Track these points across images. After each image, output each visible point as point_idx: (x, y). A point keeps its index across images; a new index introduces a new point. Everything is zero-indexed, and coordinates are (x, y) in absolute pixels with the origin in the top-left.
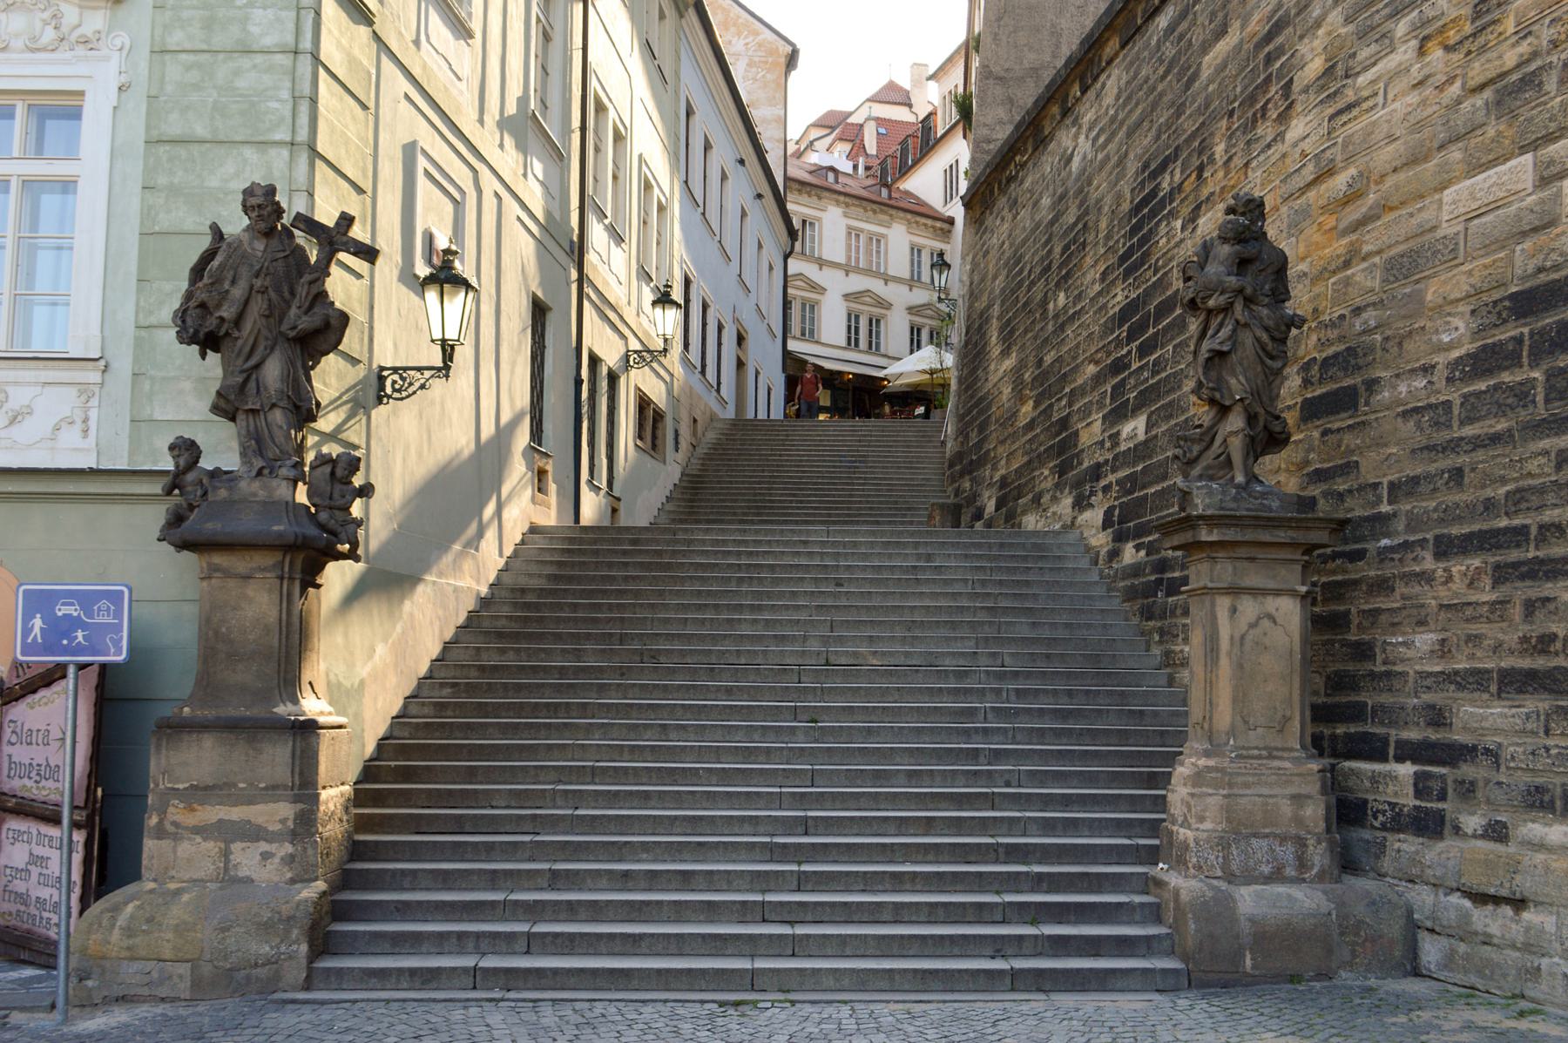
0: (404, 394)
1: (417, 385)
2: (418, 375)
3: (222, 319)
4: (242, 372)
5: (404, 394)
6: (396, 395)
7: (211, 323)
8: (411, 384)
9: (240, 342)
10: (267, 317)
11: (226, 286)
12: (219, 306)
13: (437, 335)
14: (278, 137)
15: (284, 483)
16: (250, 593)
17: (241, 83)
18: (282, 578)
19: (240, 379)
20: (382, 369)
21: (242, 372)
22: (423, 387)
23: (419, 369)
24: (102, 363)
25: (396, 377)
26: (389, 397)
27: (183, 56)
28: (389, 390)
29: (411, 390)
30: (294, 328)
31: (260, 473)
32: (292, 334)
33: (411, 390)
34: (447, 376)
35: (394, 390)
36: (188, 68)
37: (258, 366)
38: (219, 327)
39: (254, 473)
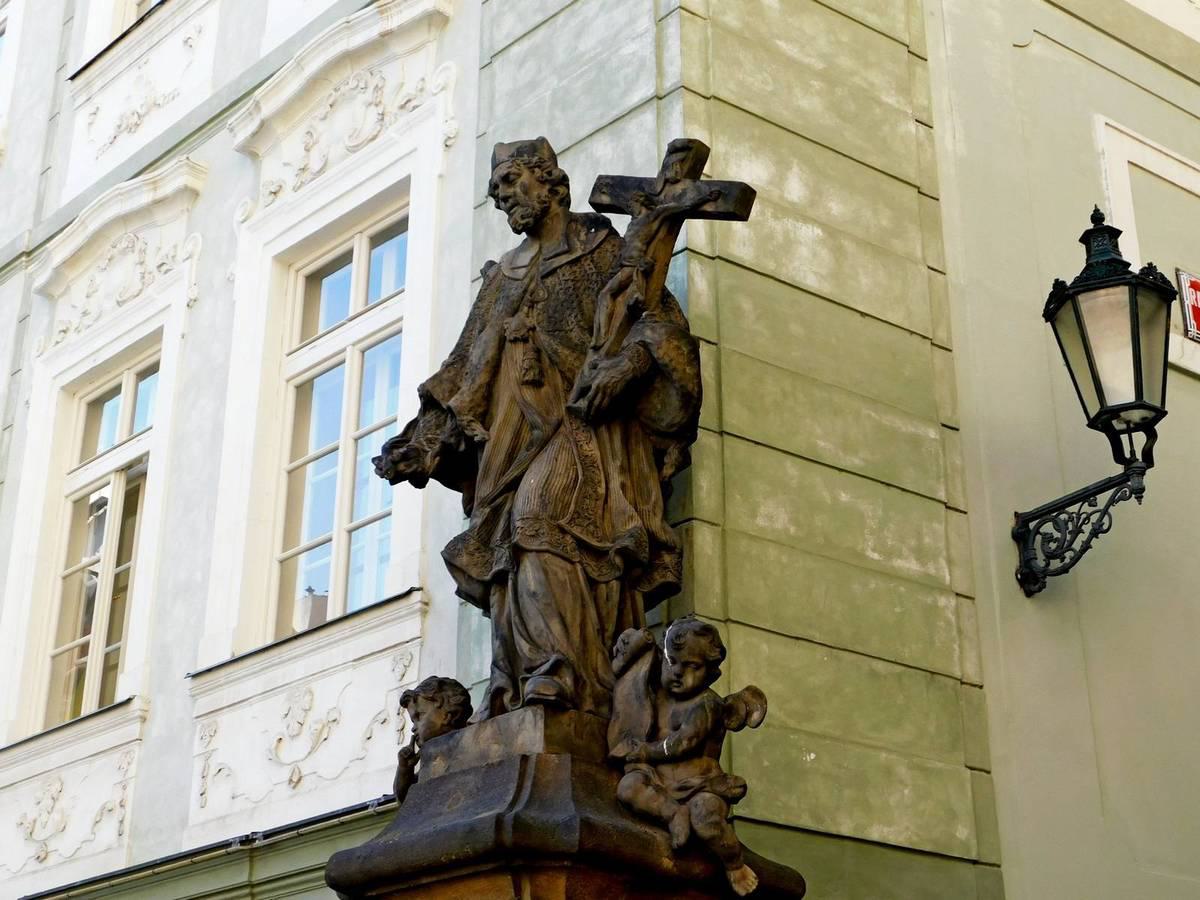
0: (1069, 555)
1: (1087, 528)
2: (1086, 508)
5: (1069, 555)
6: (1056, 564)
8: (1078, 531)
10: (536, 384)
13: (1094, 409)
14: (636, 98)
17: (587, 44)
20: (1022, 519)
22: (1096, 532)
23: (1087, 495)
24: (416, 596)
25: (1048, 528)
26: (1046, 572)
27: (516, 49)
28: (1041, 562)
29: (1077, 545)
32: (583, 404)
33: (1077, 545)
34: (1139, 492)
35: (1050, 556)
36: (521, 63)
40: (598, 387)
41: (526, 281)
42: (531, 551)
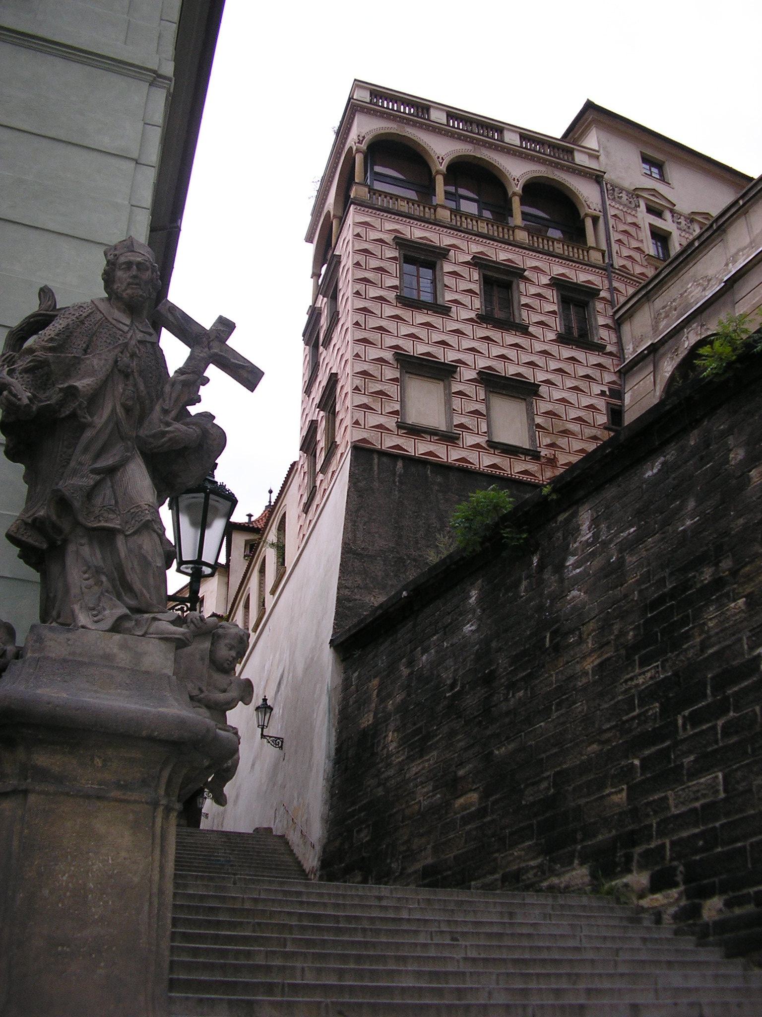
3: (72, 392)
4: (95, 471)
7: (52, 396)
9: (88, 434)
11: (76, 352)
12: (67, 375)
15: (163, 645)
16: (100, 826)
18: (155, 804)
19: (90, 481)
21: (95, 471)
30: (154, 436)
31: (116, 628)
37: (111, 471)
38: (62, 403)
39: (108, 623)
40: (170, 439)
41: (129, 336)
42: (155, 531)
